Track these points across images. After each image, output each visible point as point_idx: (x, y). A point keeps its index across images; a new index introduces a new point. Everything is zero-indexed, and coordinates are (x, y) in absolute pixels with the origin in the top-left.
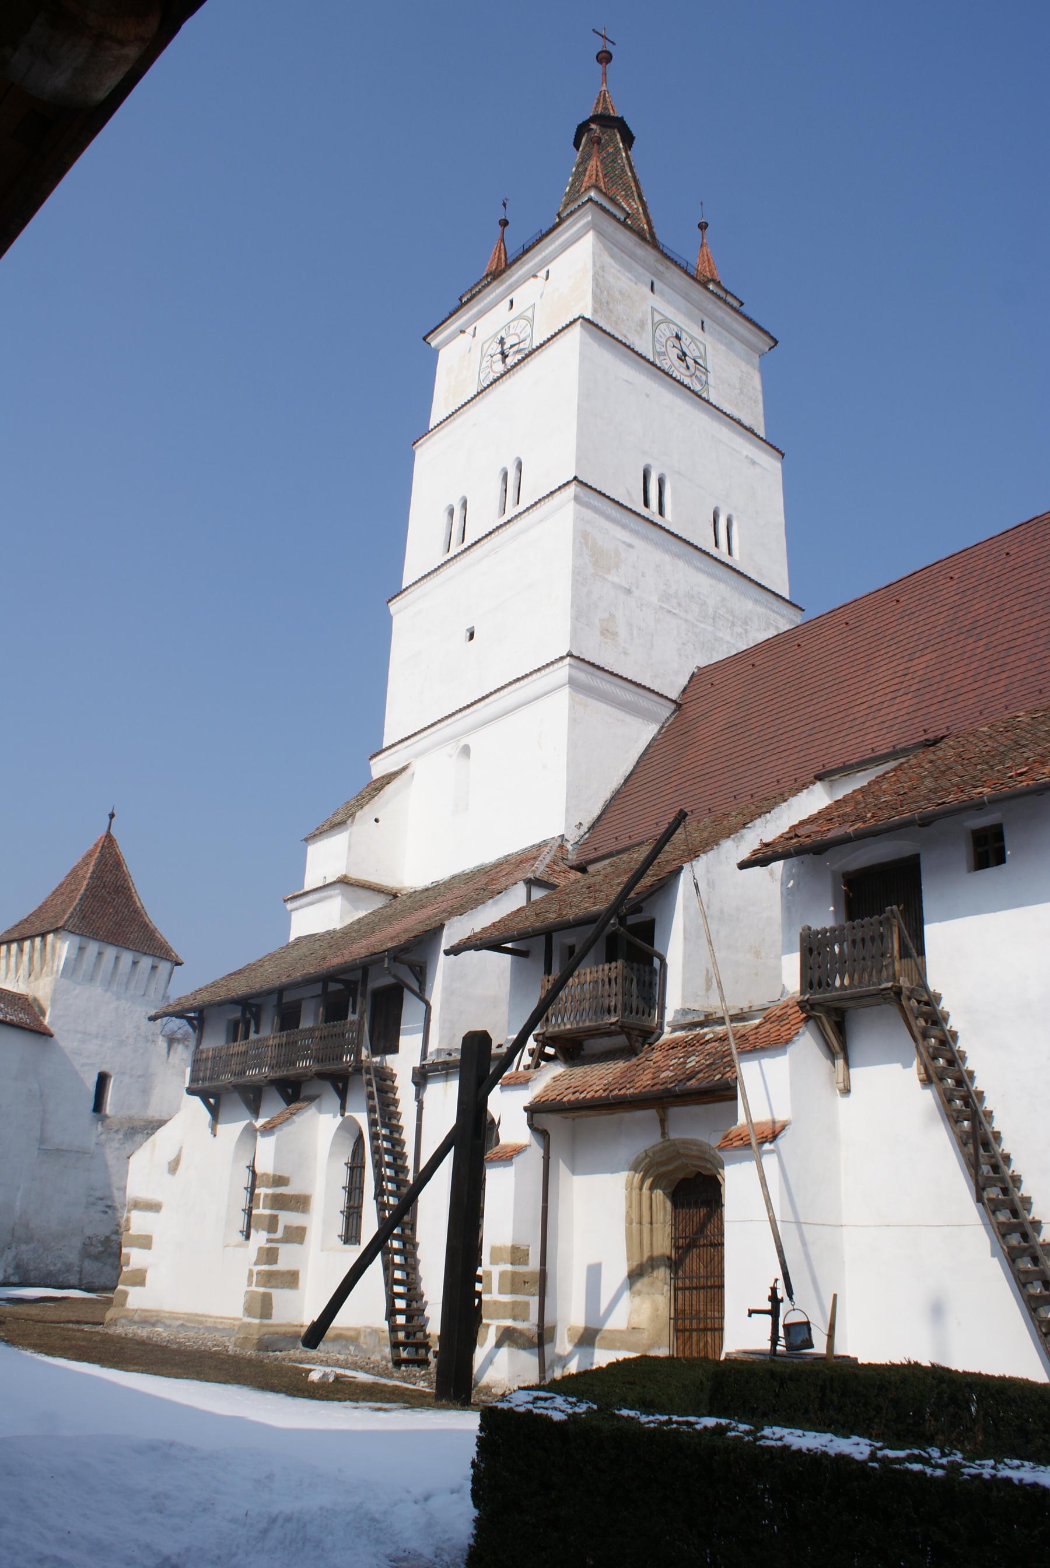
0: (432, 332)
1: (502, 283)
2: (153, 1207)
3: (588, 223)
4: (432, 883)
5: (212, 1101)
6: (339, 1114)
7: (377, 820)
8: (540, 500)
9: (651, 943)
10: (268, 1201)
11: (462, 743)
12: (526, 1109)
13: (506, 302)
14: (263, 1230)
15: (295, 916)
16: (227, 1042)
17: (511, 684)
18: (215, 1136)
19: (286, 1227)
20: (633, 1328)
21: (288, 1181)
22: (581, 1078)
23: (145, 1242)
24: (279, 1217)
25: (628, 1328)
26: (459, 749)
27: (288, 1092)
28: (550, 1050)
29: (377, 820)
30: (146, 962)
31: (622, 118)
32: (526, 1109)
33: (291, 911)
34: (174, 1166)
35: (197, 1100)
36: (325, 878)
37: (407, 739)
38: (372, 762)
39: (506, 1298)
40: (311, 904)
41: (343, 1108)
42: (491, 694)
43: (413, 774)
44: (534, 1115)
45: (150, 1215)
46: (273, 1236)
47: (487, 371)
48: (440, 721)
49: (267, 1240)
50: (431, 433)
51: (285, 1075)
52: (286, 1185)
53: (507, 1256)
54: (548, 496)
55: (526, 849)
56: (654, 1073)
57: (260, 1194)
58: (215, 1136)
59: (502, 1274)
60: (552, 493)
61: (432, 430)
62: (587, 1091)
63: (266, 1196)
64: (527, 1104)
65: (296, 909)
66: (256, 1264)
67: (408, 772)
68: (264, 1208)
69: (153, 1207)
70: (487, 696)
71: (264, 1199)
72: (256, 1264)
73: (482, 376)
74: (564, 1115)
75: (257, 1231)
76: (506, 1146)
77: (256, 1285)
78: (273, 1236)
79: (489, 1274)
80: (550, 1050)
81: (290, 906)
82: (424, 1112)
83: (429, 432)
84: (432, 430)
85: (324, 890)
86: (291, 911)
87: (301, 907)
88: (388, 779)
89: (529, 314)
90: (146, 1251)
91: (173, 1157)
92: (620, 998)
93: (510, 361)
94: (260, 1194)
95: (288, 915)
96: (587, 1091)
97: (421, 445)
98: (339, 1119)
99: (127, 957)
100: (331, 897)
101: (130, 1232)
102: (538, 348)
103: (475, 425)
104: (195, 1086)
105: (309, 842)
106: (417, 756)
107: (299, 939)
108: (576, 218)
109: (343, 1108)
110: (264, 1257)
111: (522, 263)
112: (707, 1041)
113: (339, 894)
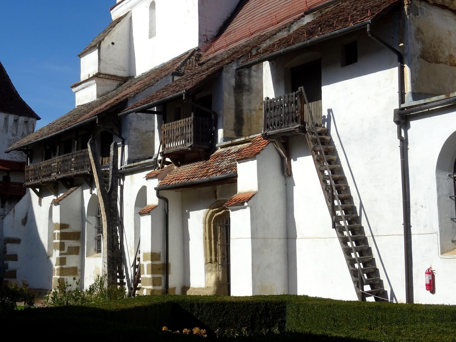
2: (17, 241)
4: (142, 74)
5: (38, 190)
7: (113, 43)
9: (210, 108)
10: (59, 236)
12: (155, 189)
14: (58, 249)
18: (41, 206)
19: (69, 247)
20: (208, 287)
21: (68, 226)
22: (179, 173)
23: (14, 258)
24: (65, 243)
25: (205, 287)
27: (68, 184)
28: (168, 160)
29: (113, 43)
30: (22, 119)
32: (155, 189)
33: (75, 92)
38: (111, 12)
39: (149, 276)
40: (83, 88)
44: (160, 191)
46: (63, 252)
49: (60, 254)
52: (67, 228)
53: (150, 257)
56: (207, 170)
57: (56, 233)
58: (41, 206)
59: (148, 265)
62: (180, 179)
63: (58, 233)
64: (156, 186)
65: (77, 91)
69: (17, 241)
74: (175, 190)
75: (56, 250)
76: (149, 206)
77: (57, 275)
78: (63, 252)
79: (143, 265)
80: (168, 160)
81: (74, 90)
86: (75, 92)
88: (119, 20)
90: (15, 262)
91: (23, 217)
92: (192, 134)
94: (56, 233)
95: (74, 94)
96: (180, 179)
99: (11, 118)
101: (7, 254)
110: (59, 262)
112: (231, 153)
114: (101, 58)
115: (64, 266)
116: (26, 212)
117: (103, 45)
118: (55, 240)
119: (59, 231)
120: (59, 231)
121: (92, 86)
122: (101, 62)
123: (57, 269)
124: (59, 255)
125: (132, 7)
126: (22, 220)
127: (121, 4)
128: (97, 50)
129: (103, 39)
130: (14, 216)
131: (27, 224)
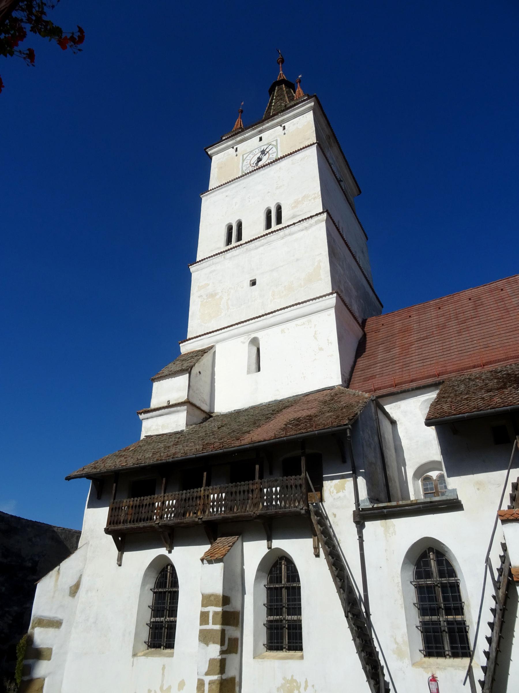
2: (56, 624)
10: (219, 618)
11: (253, 335)
14: (214, 643)
19: (229, 639)
33: (143, 420)
34: (74, 590)
35: (110, 537)
36: (169, 401)
37: (210, 333)
42: (278, 310)
45: (51, 631)
47: (248, 166)
51: (223, 517)
52: (228, 605)
61: (211, 190)
63: (216, 613)
66: (207, 674)
67: (212, 351)
68: (214, 623)
69: (56, 624)
70: (275, 312)
71: (213, 616)
72: (207, 674)
73: (244, 169)
82: (364, 543)
84: (211, 190)
86: (143, 420)
87: (152, 417)
89: (274, 143)
91: (73, 582)
93: (260, 164)
97: (207, 195)
100: (178, 411)
103: (245, 187)
104: (112, 527)
106: (217, 342)
113: (185, 410)
114: (191, 384)
115: (224, 677)
116: (78, 575)
117: (195, 371)
118: (208, 624)
119: (219, 609)
120: (219, 609)
121: (178, 413)
122: (191, 389)
123: (211, 683)
124: (218, 653)
125: (217, 342)
126: (71, 588)
127: (192, 341)
128: (188, 375)
129: (194, 365)
130: (57, 580)
131: (77, 595)
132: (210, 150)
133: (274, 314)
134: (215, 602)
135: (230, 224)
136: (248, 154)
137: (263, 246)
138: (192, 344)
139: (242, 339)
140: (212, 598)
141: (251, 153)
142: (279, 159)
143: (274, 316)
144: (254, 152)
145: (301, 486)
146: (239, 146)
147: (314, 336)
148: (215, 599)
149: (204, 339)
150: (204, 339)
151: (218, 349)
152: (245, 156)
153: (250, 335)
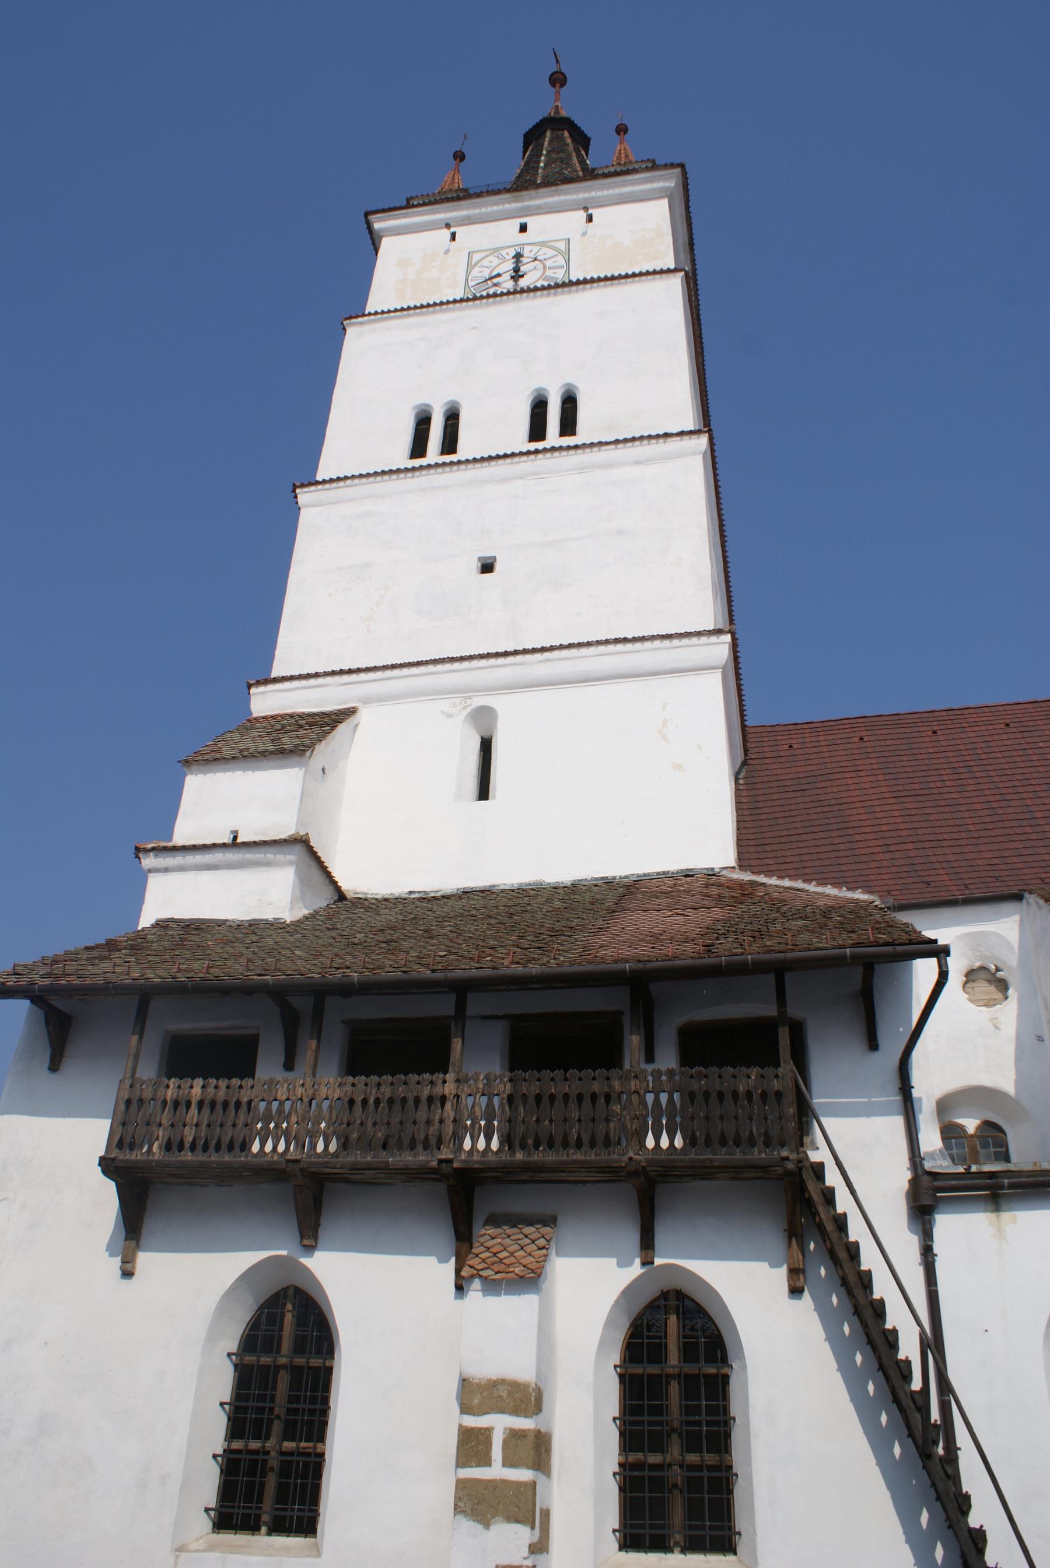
0: (383, 211)
1: (517, 200)
3: (667, 188)
4: (411, 892)
6: (638, 1261)
8: (642, 438)
11: (479, 701)
13: (516, 223)
15: (154, 883)
16: (159, 1075)
17: (607, 642)
26: (469, 710)
31: (589, 139)
33: (150, 871)
37: (350, 672)
41: (647, 1245)
42: (561, 647)
43: (357, 725)
48: (481, 657)
50: (366, 318)
54: (658, 436)
55: (645, 875)
60: (667, 435)
61: (370, 314)
70: (552, 649)
71: (505, 1443)
83: (364, 315)
84: (370, 314)
85: (257, 849)
86: (150, 871)
87: (181, 869)
89: (562, 246)
97: (362, 323)
98: (636, 1270)
100: (268, 864)
102: (578, 283)
105: (194, 768)
106: (367, 701)
107: (162, 925)
108: (661, 176)
109: (647, 1245)
111: (556, 191)
113: (291, 863)
121: (267, 868)
125: (367, 701)
127: (287, 685)
132: (380, 220)
133: (547, 655)
134: (512, 1403)
135: (423, 408)
136: (488, 253)
137: (521, 478)
138: (288, 694)
139: (445, 704)
140: (503, 1391)
141: (496, 254)
142: (571, 284)
143: (548, 660)
144: (503, 252)
145: (779, 1095)
146: (460, 231)
147: (660, 732)
148: (510, 1393)
149: (329, 685)
150: (329, 685)
151: (365, 716)
152: (476, 257)
153: (470, 698)
